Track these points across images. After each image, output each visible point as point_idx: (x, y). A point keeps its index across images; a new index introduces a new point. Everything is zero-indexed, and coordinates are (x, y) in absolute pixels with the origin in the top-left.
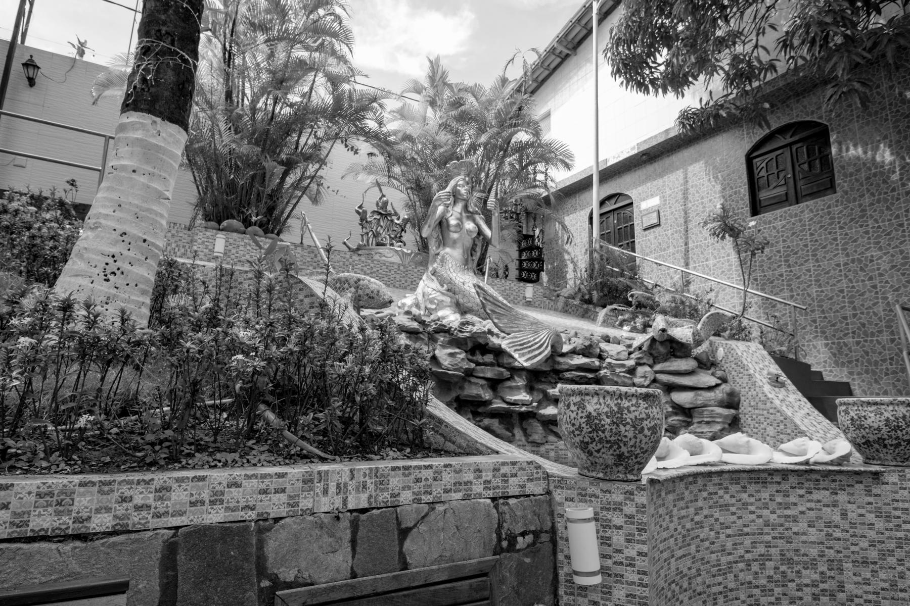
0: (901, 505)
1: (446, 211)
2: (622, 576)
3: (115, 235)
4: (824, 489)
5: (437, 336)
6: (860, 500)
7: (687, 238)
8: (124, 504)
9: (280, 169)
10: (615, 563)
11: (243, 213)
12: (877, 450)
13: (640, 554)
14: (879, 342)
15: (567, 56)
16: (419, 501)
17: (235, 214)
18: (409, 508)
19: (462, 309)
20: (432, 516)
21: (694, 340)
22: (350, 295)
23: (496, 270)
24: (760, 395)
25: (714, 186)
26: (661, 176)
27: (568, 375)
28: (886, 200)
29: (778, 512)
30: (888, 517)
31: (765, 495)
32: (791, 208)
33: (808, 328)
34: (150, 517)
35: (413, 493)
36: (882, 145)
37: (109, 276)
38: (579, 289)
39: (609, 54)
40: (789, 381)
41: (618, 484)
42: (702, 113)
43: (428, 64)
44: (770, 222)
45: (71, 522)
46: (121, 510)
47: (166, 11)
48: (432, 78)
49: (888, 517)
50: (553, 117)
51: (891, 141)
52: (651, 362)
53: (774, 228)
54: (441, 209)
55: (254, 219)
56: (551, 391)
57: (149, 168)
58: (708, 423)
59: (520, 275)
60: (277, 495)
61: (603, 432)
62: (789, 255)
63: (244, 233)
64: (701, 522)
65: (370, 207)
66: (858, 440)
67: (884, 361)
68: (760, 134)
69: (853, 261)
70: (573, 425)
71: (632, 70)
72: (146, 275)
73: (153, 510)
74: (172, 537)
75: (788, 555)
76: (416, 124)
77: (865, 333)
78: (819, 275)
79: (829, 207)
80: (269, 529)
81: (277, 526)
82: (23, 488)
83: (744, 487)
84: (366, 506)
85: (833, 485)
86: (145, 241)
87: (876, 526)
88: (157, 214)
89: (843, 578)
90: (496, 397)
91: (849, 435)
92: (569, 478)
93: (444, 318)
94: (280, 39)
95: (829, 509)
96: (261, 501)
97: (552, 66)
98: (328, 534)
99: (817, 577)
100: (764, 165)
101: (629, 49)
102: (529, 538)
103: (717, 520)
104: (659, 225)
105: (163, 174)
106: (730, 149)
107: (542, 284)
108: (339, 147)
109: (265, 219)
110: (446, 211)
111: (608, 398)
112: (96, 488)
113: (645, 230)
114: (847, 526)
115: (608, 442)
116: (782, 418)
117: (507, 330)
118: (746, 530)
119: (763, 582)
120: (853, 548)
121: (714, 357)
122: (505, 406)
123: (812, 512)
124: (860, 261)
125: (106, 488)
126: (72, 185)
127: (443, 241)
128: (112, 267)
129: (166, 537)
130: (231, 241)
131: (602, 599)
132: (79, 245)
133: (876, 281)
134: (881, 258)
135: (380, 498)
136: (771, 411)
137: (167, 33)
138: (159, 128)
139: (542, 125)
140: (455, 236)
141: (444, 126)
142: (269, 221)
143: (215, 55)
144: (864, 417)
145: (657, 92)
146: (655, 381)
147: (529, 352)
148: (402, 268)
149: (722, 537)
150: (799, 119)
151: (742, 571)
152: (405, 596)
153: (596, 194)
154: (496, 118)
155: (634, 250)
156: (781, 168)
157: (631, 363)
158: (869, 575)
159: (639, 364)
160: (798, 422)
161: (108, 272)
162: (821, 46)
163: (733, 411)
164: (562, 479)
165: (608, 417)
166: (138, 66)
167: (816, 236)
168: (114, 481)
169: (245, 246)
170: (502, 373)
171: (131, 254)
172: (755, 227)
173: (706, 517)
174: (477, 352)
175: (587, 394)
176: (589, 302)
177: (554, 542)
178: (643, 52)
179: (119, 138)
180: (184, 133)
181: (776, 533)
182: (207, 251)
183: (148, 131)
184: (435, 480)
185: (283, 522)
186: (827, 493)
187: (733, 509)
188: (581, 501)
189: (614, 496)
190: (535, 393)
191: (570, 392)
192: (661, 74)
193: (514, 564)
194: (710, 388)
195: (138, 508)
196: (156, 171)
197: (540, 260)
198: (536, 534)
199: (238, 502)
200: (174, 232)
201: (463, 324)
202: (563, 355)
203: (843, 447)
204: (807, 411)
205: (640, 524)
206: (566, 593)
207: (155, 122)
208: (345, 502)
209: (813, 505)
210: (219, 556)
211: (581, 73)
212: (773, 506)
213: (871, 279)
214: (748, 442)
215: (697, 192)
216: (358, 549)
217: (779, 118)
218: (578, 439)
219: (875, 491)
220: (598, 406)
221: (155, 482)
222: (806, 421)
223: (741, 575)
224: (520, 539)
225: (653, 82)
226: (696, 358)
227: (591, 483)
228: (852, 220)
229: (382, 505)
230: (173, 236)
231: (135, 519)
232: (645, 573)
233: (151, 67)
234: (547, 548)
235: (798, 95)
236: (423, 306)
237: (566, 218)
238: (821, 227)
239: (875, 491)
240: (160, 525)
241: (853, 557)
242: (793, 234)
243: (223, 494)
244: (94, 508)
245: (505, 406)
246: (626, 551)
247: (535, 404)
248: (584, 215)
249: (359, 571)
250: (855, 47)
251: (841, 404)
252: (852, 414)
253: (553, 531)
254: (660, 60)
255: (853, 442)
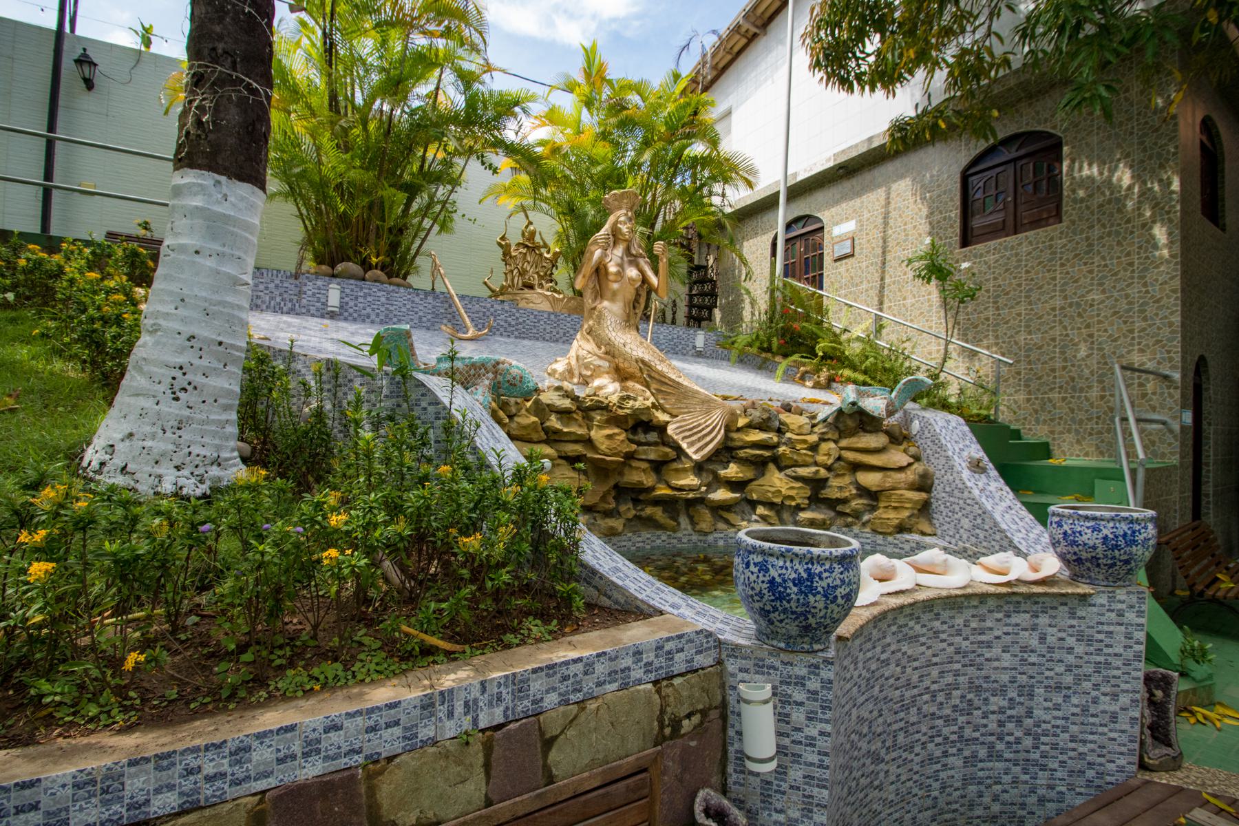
0: (1105, 628)
1: (604, 255)
2: (800, 756)
3: (181, 340)
4: (1025, 612)
5: (593, 414)
6: (1062, 623)
7: (883, 272)
8: (191, 778)
9: (402, 196)
10: (793, 742)
11: (360, 253)
12: (1089, 569)
13: (822, 733)
14: (1087, 399)
15: (755, 35)
16: (566, 703)
17: (351, 253)
18: (553, 714)
19: (622, 375)
20: (583, 717)
21: (887, 411)
22: (487, 382)
23: (663, 312)
24: (957, 482)
25: (920, 210)
26: (859, 194)
27: (741, 453)
28: (1118, 233)
29: (971, 638)
30: (1090, 641)
31: (959, 621)
32: (1008, 239)
33: (1011, 380)
34: (226, 787)
35: (560, 694)
36: (1121, 165)
37: (178, 394)
38: (757, 337)
39: (808, 41)
40: (991, 465)
41: (801, 656)
42: (917, 124)
43: (583, 51)
44: (981, 255)
45: (124, 810)
46: (187, 785)
47: (221, 20)
48: (588, 74)
49: (1090, 641)
50: (734, 116)
51: (1133, 161)
52: (836, 436)
53: (986, 263)
54: (598, 253)
55: (374, 260)
56: (722, 472)
57: (217, 247)
58: (895, 508)
59: (690, 312)
60: (389, 730)
61: (789, 602)
62: (998, 296)
63: (364, 279)
64: (888, 659)
65: (515, 238)
66: (1068, 556)
67: (1089, 419)
68: (983, 145)
69: (1071, 305)
70: (753, 589)
71: (834, 62)
72: (226, 386)
73: (229, 777)
74: (258, 804)
75: (977, 682)
76: (569, 131)
77: (1074, 389)
78: (1031, 320)
79: (1052, 239)
80: (381, 772)
81: (391, 766)
82: (54, 781)
83: (938, 614)
84: (502, 720)
85: (1034, 608)
86: (220, 344)
87: (1076, 650)
88: (232, 306)
89: (1033, 704)
90: (660, 480)
91: (1058, 550)
92: (745, 647)
93: (600, 388)
94: (390, 24)
95: (1027, 634)
96: (369, 741)
97: (736, 49)
98: (455, 762)
99: (1005, 703)
100: (981, 184)
101: (833, 34)
102: (696, 719)
103: (905, 653)
104: (853, 255)
105: (237, 253)
106: (944, 164)
107: (714, 329)
108: (474, 165)
109: (388, 259)
110: (604, 255)
111: (796, 562)
112: (152, 765)
113: (836, 261)
114: (1044, 651)
115: (793, 613)
116: (980, 512)
117: (675, 412)
118: (935, 660)
119: (947, 711)
120: (1047, 673)
121: (907, 429)
122: (669, 492)
123: (1008, 637)
124: (1078, 305)
125: (165, 763)
126: (146, 228)
127: (600, 293)
128: (181, 381)
129: (249, 806)
130: (347, 291)
131: (776, 779)
132: (138, 352)
133: (1093, 330)
134: (1103, 302)
135: (519, 709)
136: (969, 501)
137: (226, 52)
138: (225, 190)
139: (719, 128)
140: (615, 286)
141: (604, 136)
142: (393, 261)
143: (314, 45)
144: (1080, 532)
145: (863, 89)
146: (839, 459)
147: (699, 440)
148: (552, 317)
149: (909, 670)
150: (1029, 129)
151: (926, 702)
152: (550, 814)
153: (782, 215)
154: (666, 123)
155: (821, 288)
156: (1001, 189)
157: (813, 438)
158: (1060, 700)
159: (822, 440)
160: (999, 519)
161: (176, 388)
162: (1070, 38)
163: (924, 495)
164: (737, 647)
165: (795, 585)
166: (190, 102)
167: (1032, 275)
168: (175, 752)
169: (365, 297)
170: (667, 454)
171: (204, 362)
172: (969, 269)
173: (893, 653)
174: (640, 430)
175: (772, 555)
176: (769, 350)
177: (724, 718)
178: (850, 38)
179: (173, 206)
180: (260, 192)
182: (319, 305)
183: (210, 195)
184: (586, 673)
185: (398, 760)
186: (1027, 616)
187: (923, 640)
188: (757, 673)
189: (796, 669)
190: (704, 475)
191: (750, 548)
192: (870, 66)
193: (677, 751)
194: (901, 469)
195: (209, 779)
196: (226, 250)
197: (713, 295)
198: (704, 713)
199: (339, 748)
200: (277, 282)
201: (623, 398)
202: (739, 430)
203: (1051, 565)
204: (1009, 503)
205: (823, 701)
206: (735, 771)
207: (219, 182)
208: (475, 721)
209: (1010, 629)
210: (319, 817)
211: (771, 58)
213: (1088, 326)
214: (946, 560)
215: (900, 216)
216: (493, 773)
217: (1005, 126)
218: (757, 605)
219: (1079, 613)
220: (784, 571)
221: (229, 744)
222: (1007, 516)
223: (925, 707)
224: (686, 723)
225: (858, 77)
226: (887, 433)
227: (770, 654)
228: (1076, 256)
229: (522, 715)
230: (277, 286)
231: (208, 791)
232: (826, 754)
233: (207, 104)
234: (716, 726)
235: (1031, 97)
236: (576, 372)
237: (745, 244)
238: (1040, 263)
239: (1079, 613)
240: (242, 793)
241: (1046, 682)
242: (1007, 270)
243: (318, 741)
244: (151, 788)
245: (669, 492)
246: (806, 730)
247: (703, 489)
248: (768, 238)
249: (495, 798)
250: (1110, 40)
251: (1054, 514)
252: (1066, 527)
253: (724, 704)
254: (870, 48)
255: (1062, 557)
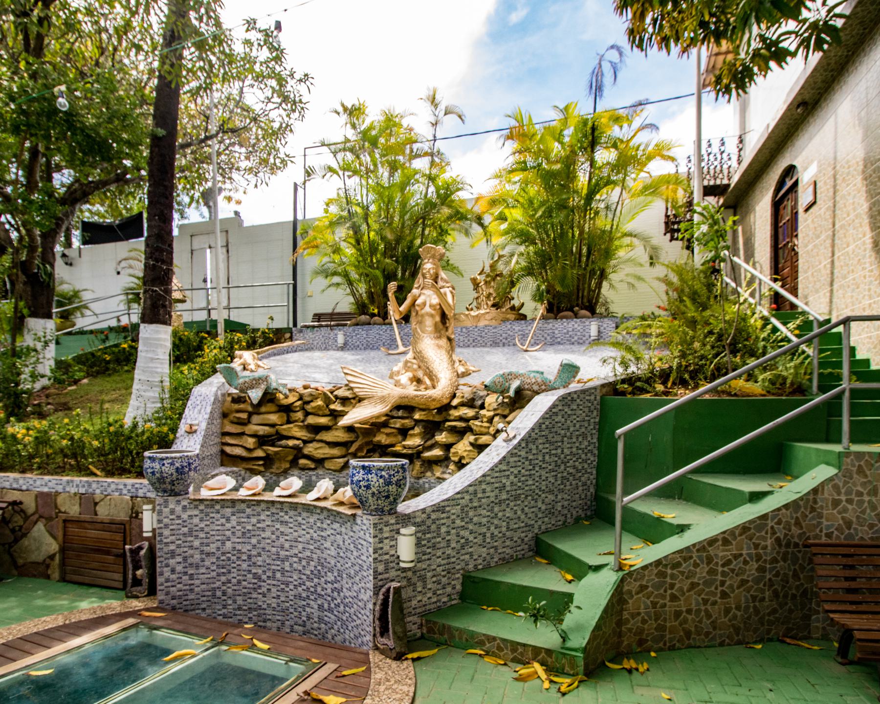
31: (312, 520)
118: (300, 539)
119: (308, 573)
181: (316, 545)
212: (315, 528)
